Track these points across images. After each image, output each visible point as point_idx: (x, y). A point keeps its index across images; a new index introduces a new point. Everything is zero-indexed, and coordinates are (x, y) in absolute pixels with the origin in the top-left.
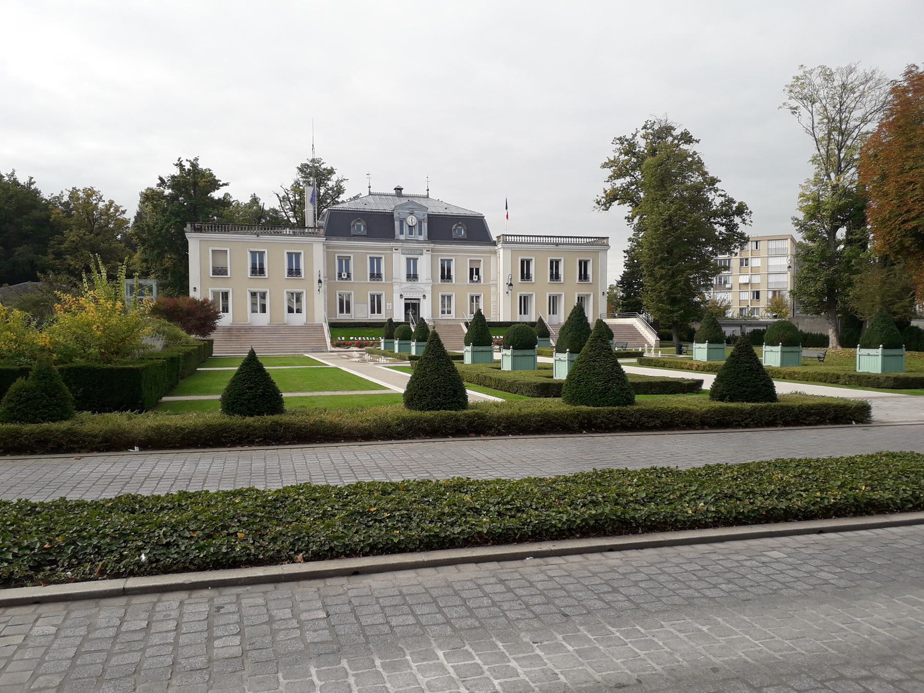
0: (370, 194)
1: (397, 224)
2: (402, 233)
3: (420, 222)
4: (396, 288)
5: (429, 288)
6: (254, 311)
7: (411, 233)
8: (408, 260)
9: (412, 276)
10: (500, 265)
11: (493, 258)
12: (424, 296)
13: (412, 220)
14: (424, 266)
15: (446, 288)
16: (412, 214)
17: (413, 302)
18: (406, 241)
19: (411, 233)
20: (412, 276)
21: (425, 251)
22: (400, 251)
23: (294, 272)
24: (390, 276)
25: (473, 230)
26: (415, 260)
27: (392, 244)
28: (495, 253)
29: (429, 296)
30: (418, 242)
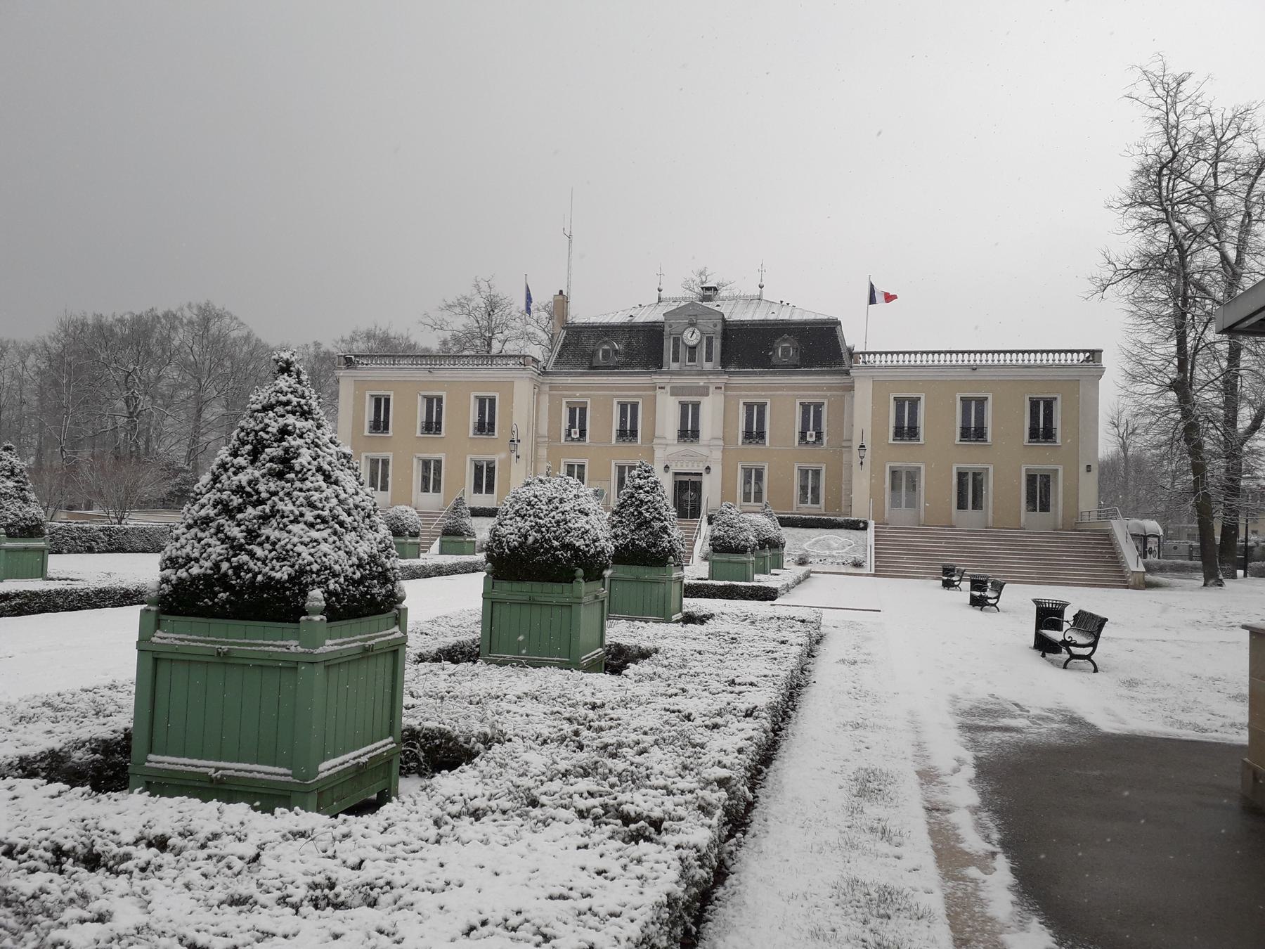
0: (660, 300)
1: (668, 345)
2: (676, 359)
3: (710, 340)
4: (659, 453)
5: (717, 455)
6: (425, 489)
7: (692, 359)
8: (684, 406)
9: (689, 433)
10: (865, 413)
11: (847, 398)
12: (708, 468)
13: (691, 338)
14: (711, 412)
15: (754, 456)
16: (693, 325)
17: (694, 478)
18: (679, 373)
19: (692, 359)
20: (689, 433)
21: (712, 389)
22: (668, 389)
23: (485, 427)
24: (652, 436)
25: (819, 345)
26: (696, 406)
27: (658, 379)
28: (850, 388)
29: (717, 470)
30: (702, 373)
